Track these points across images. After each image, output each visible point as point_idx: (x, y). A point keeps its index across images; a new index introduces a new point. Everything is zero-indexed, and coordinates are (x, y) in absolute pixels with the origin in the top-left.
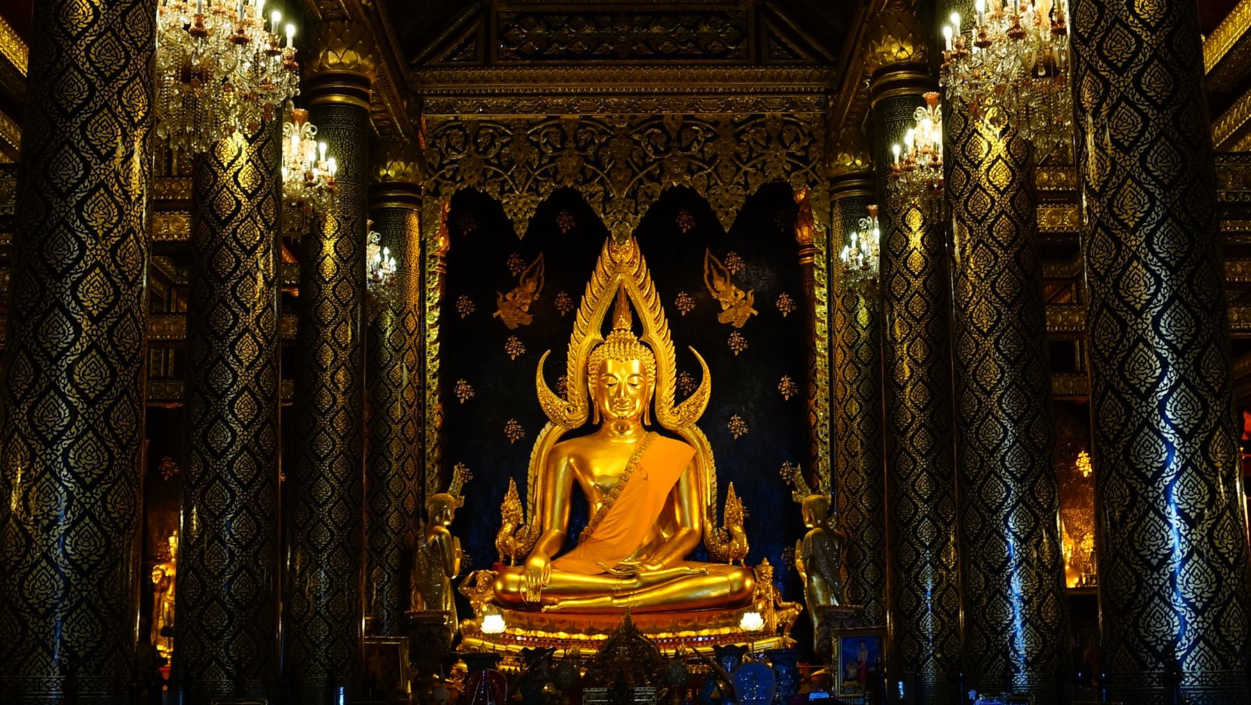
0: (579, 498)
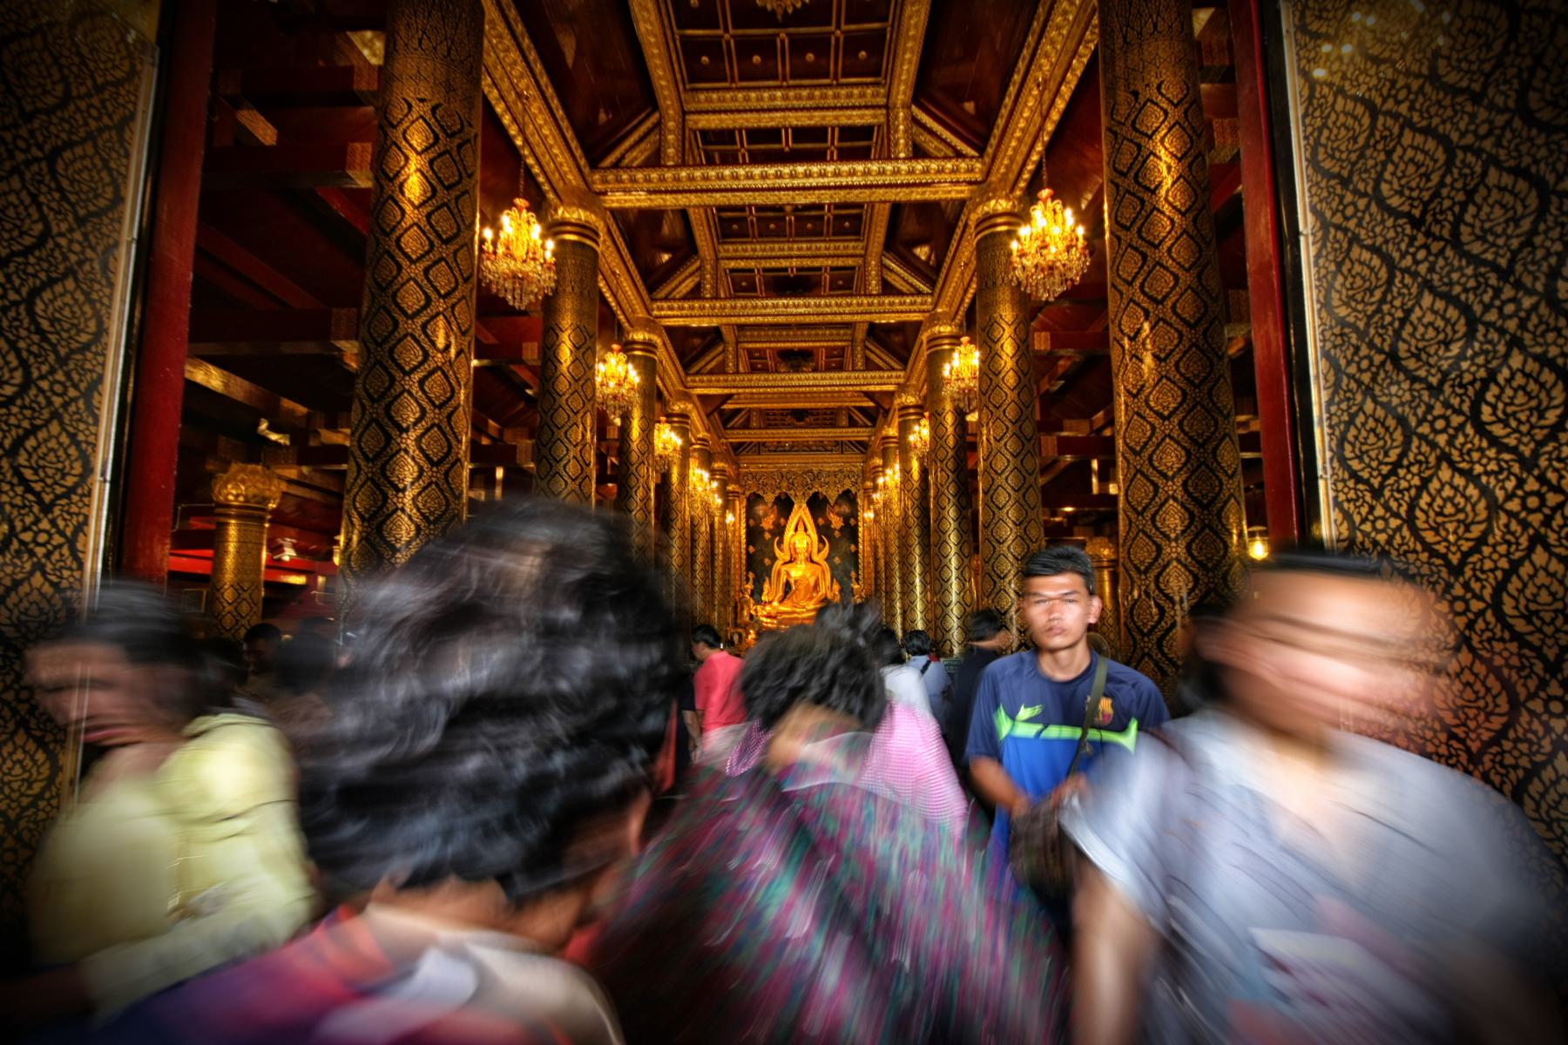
0: (788, 584)
